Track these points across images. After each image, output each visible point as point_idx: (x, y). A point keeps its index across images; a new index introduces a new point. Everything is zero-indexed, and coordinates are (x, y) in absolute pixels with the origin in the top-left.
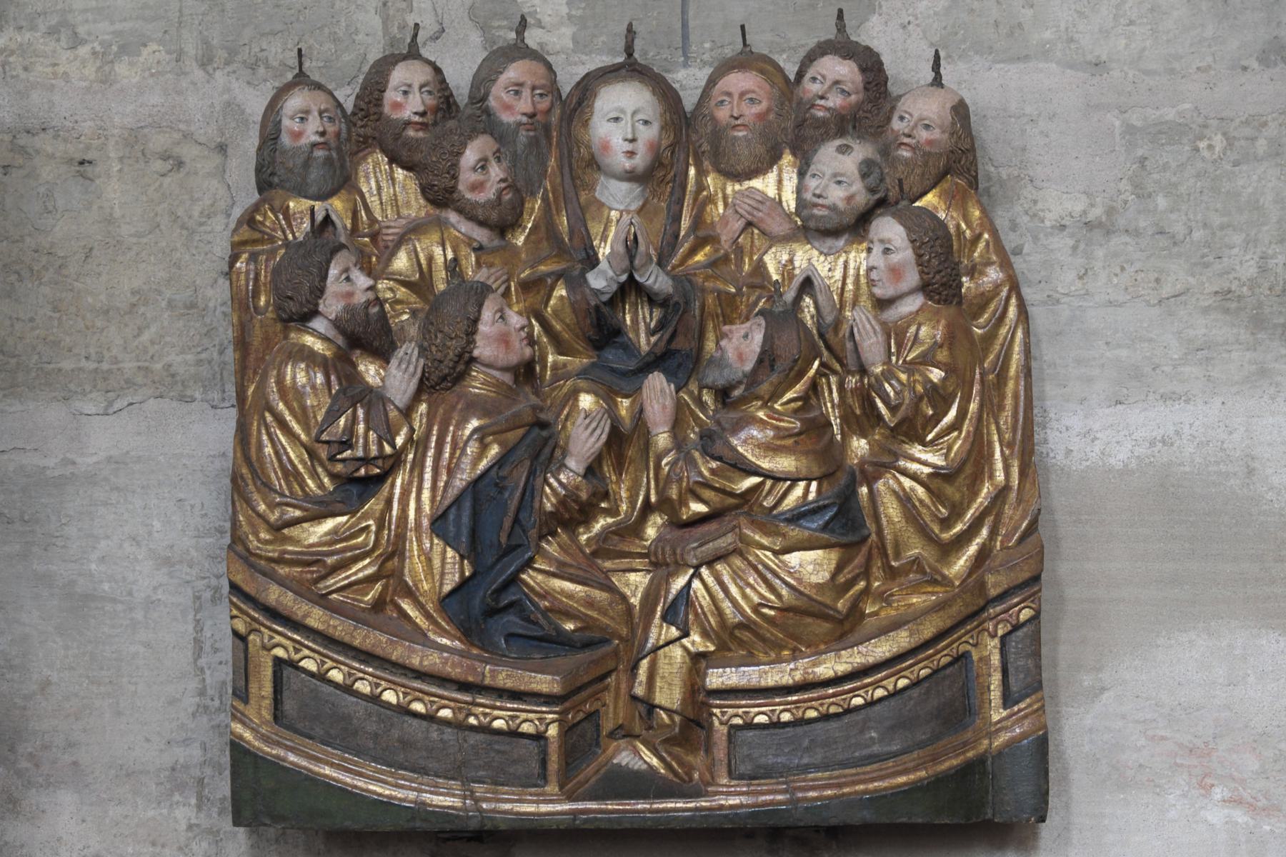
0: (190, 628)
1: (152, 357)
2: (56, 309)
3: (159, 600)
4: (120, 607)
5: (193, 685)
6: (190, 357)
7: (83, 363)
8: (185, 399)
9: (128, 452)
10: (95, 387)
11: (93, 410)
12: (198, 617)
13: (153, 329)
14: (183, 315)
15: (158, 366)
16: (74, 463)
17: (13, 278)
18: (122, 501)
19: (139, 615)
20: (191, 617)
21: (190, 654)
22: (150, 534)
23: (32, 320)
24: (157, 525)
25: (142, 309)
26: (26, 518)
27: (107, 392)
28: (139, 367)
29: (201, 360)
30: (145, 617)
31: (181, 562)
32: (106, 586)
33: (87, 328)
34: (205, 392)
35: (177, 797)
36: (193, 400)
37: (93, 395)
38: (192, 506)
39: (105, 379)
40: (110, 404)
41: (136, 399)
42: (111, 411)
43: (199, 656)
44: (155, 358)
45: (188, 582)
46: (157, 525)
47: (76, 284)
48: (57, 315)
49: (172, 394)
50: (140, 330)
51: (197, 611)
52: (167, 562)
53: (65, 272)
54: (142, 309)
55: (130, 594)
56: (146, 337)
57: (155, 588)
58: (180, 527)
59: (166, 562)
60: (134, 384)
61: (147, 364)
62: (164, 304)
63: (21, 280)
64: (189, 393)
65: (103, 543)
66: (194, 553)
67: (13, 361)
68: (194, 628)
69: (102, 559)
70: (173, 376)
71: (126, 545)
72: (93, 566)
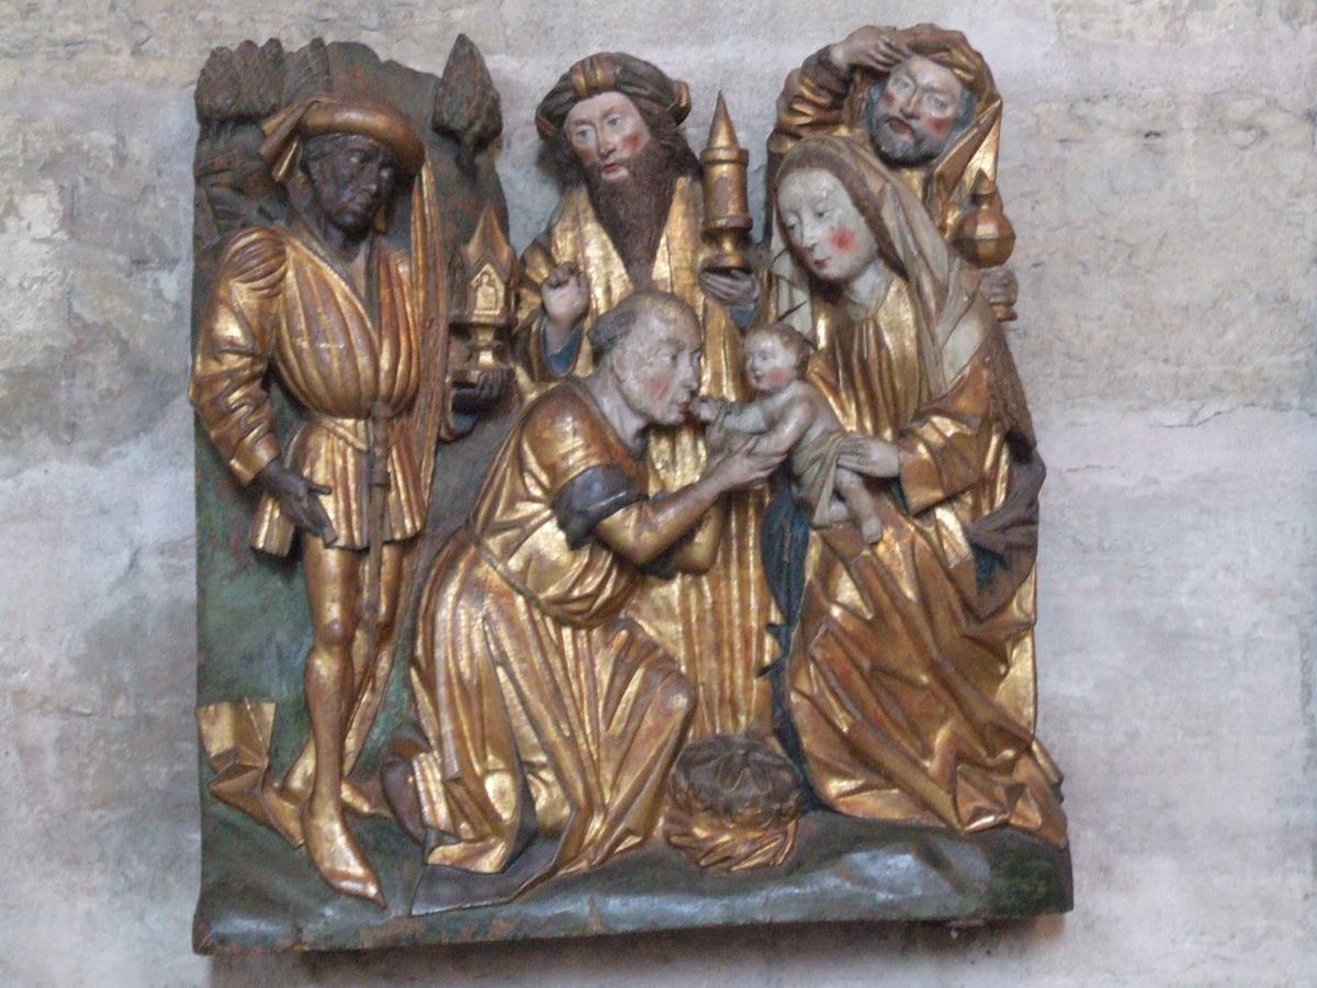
0: (1297, 672)
1: (1240, 359)
2: (1128, 306)
3: (1261, 638)
4: (1216, 647)
5: (1302, 734)
6: (1284, 359)
7: (1162, 367)
8: (1279, 407)
9: (1217, 469)
10: (1176, 394)
11: (1176, 421)
12: (1305, 657)
13: (1240, 327)
14: (1272, 310)
15: (1247, 370)
16: (1156, 482)
17: (1078, 269)
18: (1212, 524)
19: (1238, 655)
20: (1297, 658)
21: (1297, 700)
22: (1246, 562)
23: (1100, 318)
24: (1254, 552)
25: (1226, 305)
26: (1106, 545)
27: (1191, 399)
28: (1225, 372)
29: (1297, 362)
30: (1245, 658)
31: (1282, 594)
32: (1199, 623)
33: (1165, 327)
34: (1302, 398)
35: (1290, 863)
36: (1289, 407)
37: (1176, 403)
38: (1294, 530)
39: (1189, 385)
40: (1195, 413)
41: (1224, 407)
42: (1196, 422)
43: (1308, 702)
44: (1244, 360)
45: (1291, 617)
46: (1254, 552)
47: (1148, 276)
48: (1129, 312)
49: (1264, 402)
50: (1225, 327)
51: (1303, 651)
52: (1266, 595)
53: (1135, 261)
54: (1226, 305)
55: (1227, 631)
56: (1231, 336)
57: (1255, 625)
58: (1281, 554)
59: (1266, 595)
60: (1220, 390)
61: (1233, 367)
62: (1251, 297)
63: (1086, 270)
64: (1284, 399)
65: (1194, 575)
66: (1297, 584)
67: (1080, 366)
68: (1302, 669)
69: (1193, 593)
70: (1266, 380)
71: (1220, 576)
72: (1184, 600)
